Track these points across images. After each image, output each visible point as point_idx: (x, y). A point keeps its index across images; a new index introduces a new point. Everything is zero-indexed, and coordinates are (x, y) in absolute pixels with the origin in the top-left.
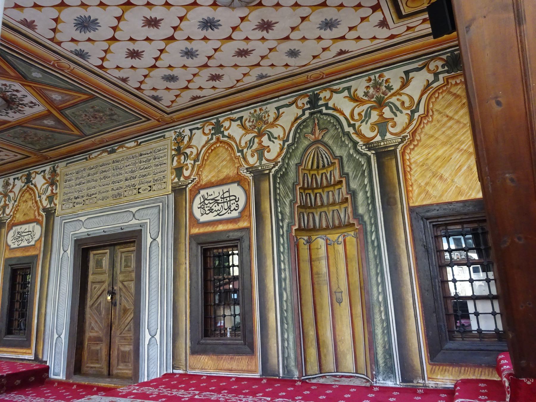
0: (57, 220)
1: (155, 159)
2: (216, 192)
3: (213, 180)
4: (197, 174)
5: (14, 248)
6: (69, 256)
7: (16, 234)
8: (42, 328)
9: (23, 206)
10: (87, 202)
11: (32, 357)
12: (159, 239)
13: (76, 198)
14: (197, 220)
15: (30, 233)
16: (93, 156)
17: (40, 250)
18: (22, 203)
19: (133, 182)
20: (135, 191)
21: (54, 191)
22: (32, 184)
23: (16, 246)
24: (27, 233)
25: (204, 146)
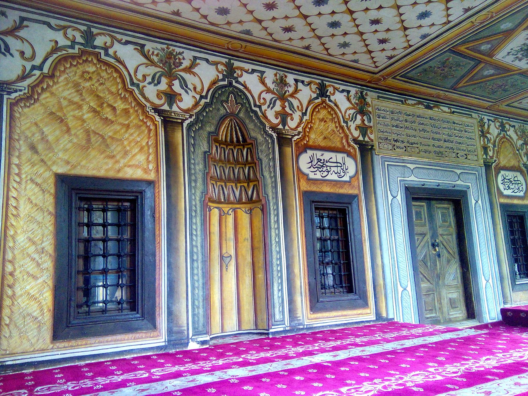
0: (378, 160)
1: (466, 131)
2: (510, 175)
3: (507, 165)
4: (497, 157)
5: (312, 180)
6: (400, 203)
7: (316, 161)
8: (381, 282)
9: (318, 126)
10: (409, 149)
11: (373, 317)
12: (480, 202)
13: (396, 141)
14: (502, 193)
15: (339, 165)
16: (409, 102)
17: (359, 189)
18: (318, 122)
19: (450, 145)
20: (454, 155)
21: (366, 122)
22: (330, 101)
23: (318, 176)
24: (336, 165)
25: (497, 137)
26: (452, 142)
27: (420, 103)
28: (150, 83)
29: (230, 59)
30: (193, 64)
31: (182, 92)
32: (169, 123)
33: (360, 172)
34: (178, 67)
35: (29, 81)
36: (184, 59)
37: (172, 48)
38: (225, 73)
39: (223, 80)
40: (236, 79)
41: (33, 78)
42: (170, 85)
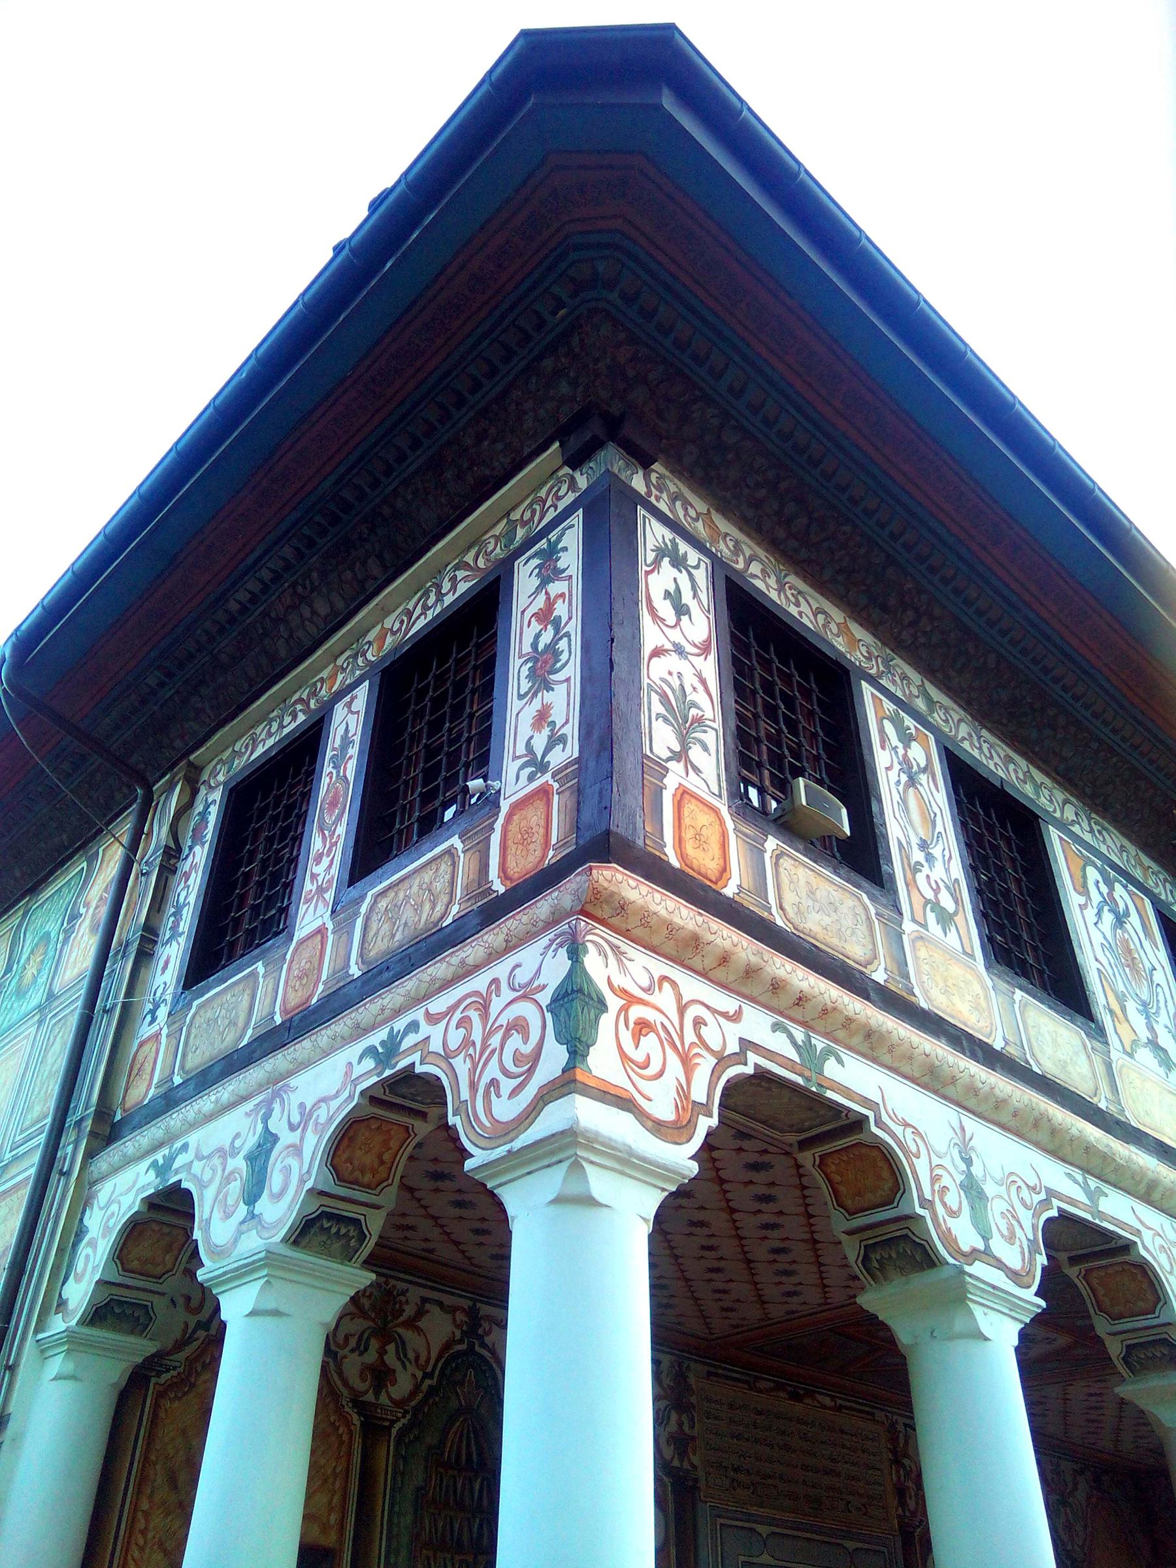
16: (762, 1385)
21: (686, 1428)
26: (838, 1475)
27: (779, 1387)
28: (353, 1351)
29: (475, 1301)
30: (420, 1313)
31: (397, 1365)
32: (373, 1429)
33: (672, 1541)
34: (398, 1317)
35: (188, 1351)
36: (407, 1302)
37: (393, 1282)
38: (465, 1328)
39: (461, 1341)
40: (480, 1338)
41: (196, 1344)
42: (382, 1352)
